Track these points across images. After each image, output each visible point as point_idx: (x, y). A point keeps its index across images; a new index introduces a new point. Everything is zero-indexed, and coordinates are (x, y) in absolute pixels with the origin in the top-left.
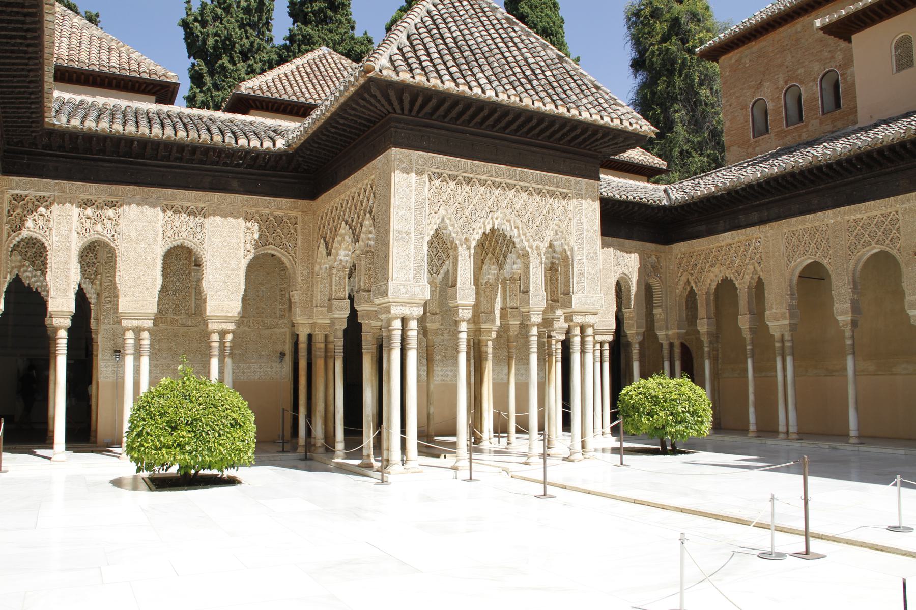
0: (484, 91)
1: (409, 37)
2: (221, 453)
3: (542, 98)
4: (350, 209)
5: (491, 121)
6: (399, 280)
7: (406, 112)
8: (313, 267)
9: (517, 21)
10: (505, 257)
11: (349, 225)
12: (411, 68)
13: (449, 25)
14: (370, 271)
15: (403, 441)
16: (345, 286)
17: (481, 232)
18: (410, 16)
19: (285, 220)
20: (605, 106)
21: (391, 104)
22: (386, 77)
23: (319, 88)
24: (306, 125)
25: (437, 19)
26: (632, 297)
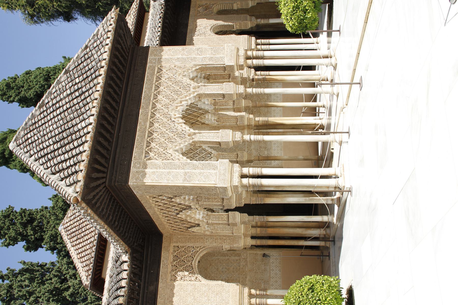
0: (90, 124)
1: (54, 174)
2: (331, 299)
3: (94, 85)
4: (169, 211)
5: (110, 119)
6: (216, 179)
7: (105, 175)
8: (205, 235)
9: (41, 101)
10: (200, 109)
11: (179, 212)
12: (75, 172)
13: (45, 146)
14: (210, 199)
15: (323, 177)
16: (219, 215)
17: (184, 126)
18: (39, 172)
19: (175, 254)
20: (98, 42)
21: (99, 185)
22: (81, 189)
23: (88, 232)
24: (113, 241)
26: (226, 23)
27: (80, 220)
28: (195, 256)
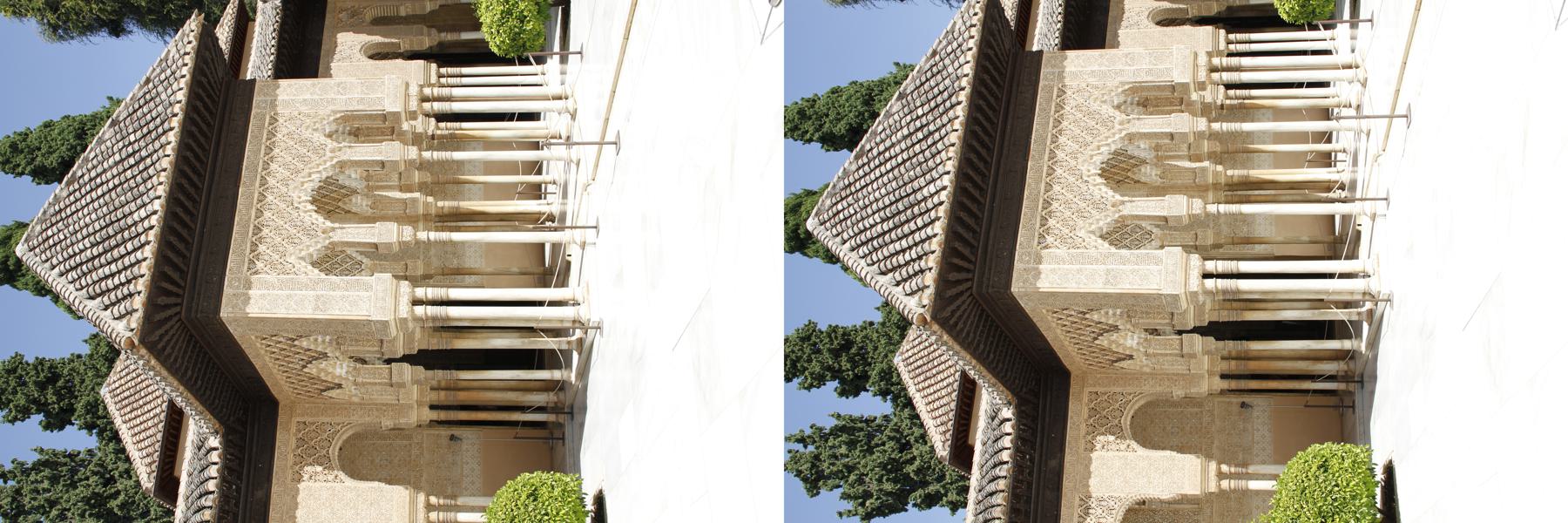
0: (155, 212)
1: (92, 298)
3: (162, 146)
5: (188, 204)
9: (71, 172)
10: (343, 187)
12: (128, 295)
13: (77, 251)
17: (315, 215)
18: (66, 296)
20: (169, 72)
21: (170, 318)
23: (150, 397)
24: (194, 413)
25: (70, 265)
26: (387, 40)
27: (138, 377)
28: (333, 439)
